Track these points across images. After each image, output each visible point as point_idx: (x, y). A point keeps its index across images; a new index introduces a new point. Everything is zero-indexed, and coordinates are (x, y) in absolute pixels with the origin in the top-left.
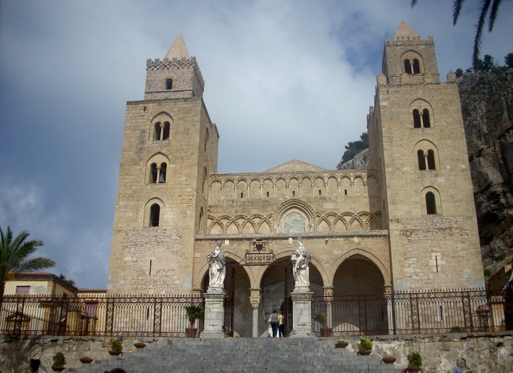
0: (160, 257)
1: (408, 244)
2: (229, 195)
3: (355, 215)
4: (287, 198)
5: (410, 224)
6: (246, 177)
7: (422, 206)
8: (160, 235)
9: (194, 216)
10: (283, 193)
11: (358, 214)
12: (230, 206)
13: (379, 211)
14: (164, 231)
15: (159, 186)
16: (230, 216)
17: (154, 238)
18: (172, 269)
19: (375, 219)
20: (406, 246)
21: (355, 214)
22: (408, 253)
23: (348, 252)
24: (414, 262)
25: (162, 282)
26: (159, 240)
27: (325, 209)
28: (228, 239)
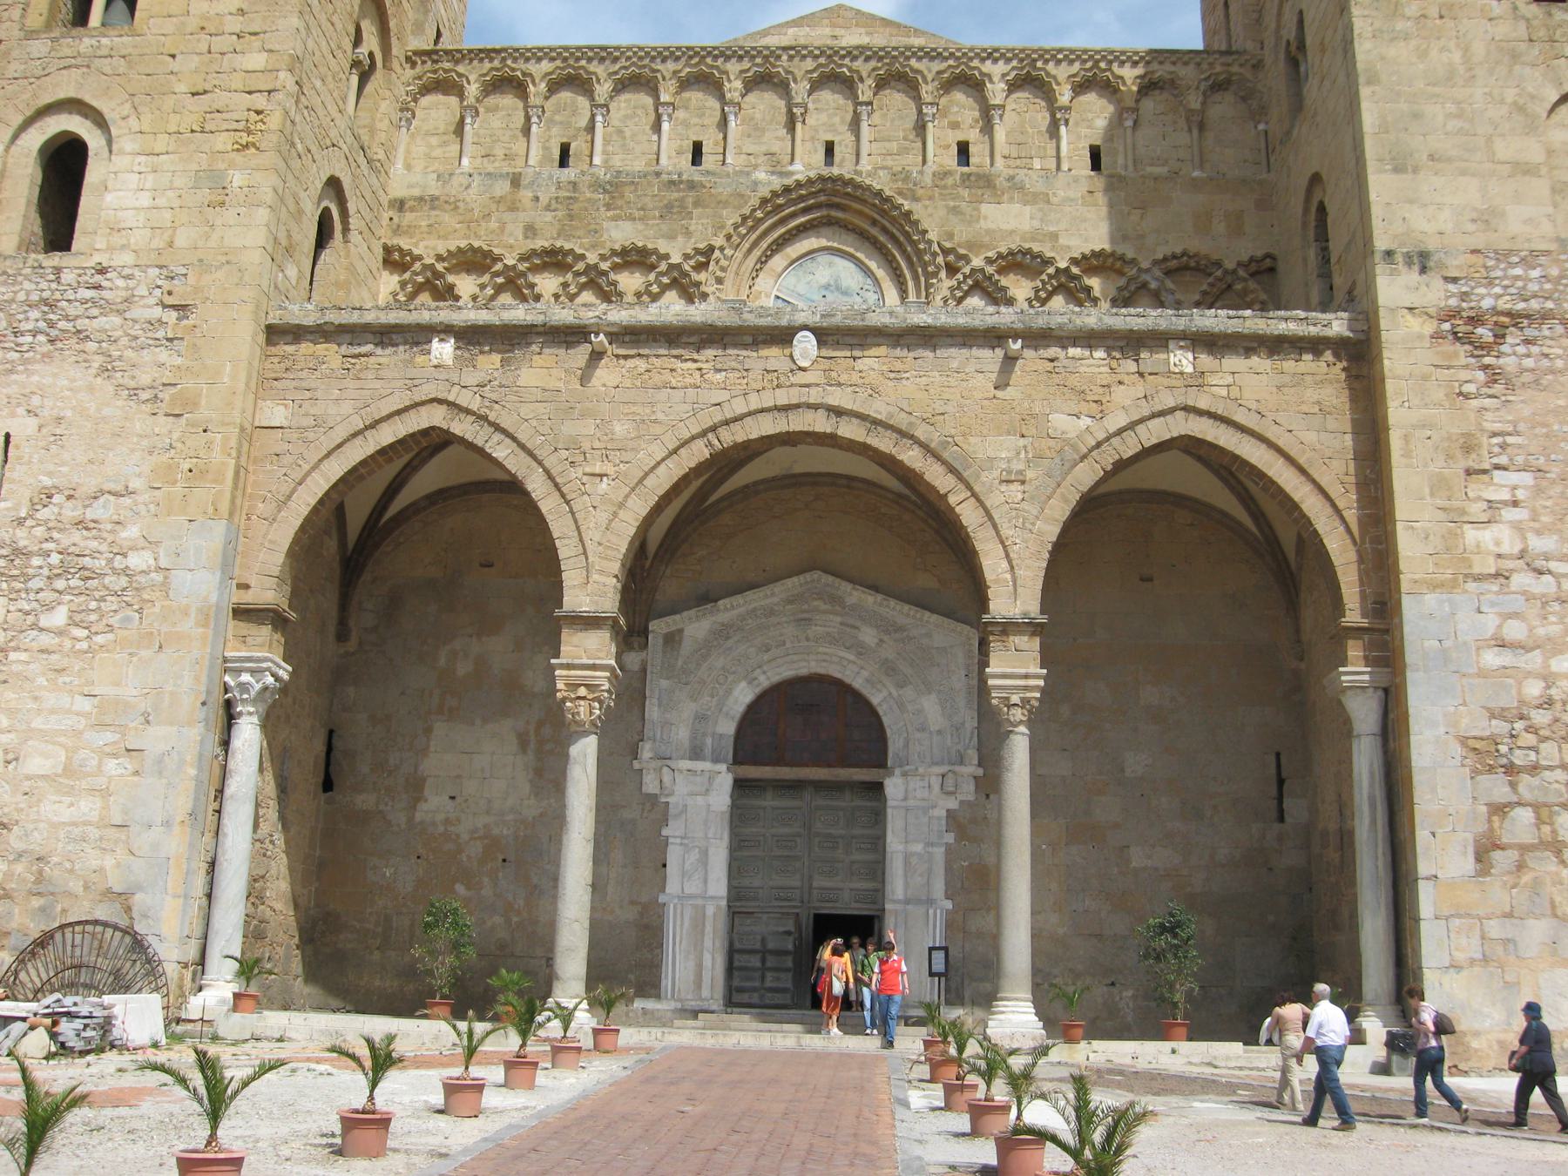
0: (59, 420)
1: (1485, 390)
2: (499, 152)
3: (1140, 270)
4: (792, 173)
5: (1490, 282)
6: (593, 67)
7: (1554, 190)
8: (70, 295)
9: (269, 197)
10: (775, 148)
11: (1156, 262)
12: (499, 201)
13: (1268, 256)
14: (98, 278)
15: (94, 42)
16: (496, 251)
17: (35, 314)
18: (119, 488)
19: (1245, 292)
20: (1474, 403)
21: (1145, 265)
22: (1485, 440)
23: (1132, 426)
24: (1521, 494)
25: (55, 559)
26: (62, 324)
27: (988, 232)
28: (446, 330)
